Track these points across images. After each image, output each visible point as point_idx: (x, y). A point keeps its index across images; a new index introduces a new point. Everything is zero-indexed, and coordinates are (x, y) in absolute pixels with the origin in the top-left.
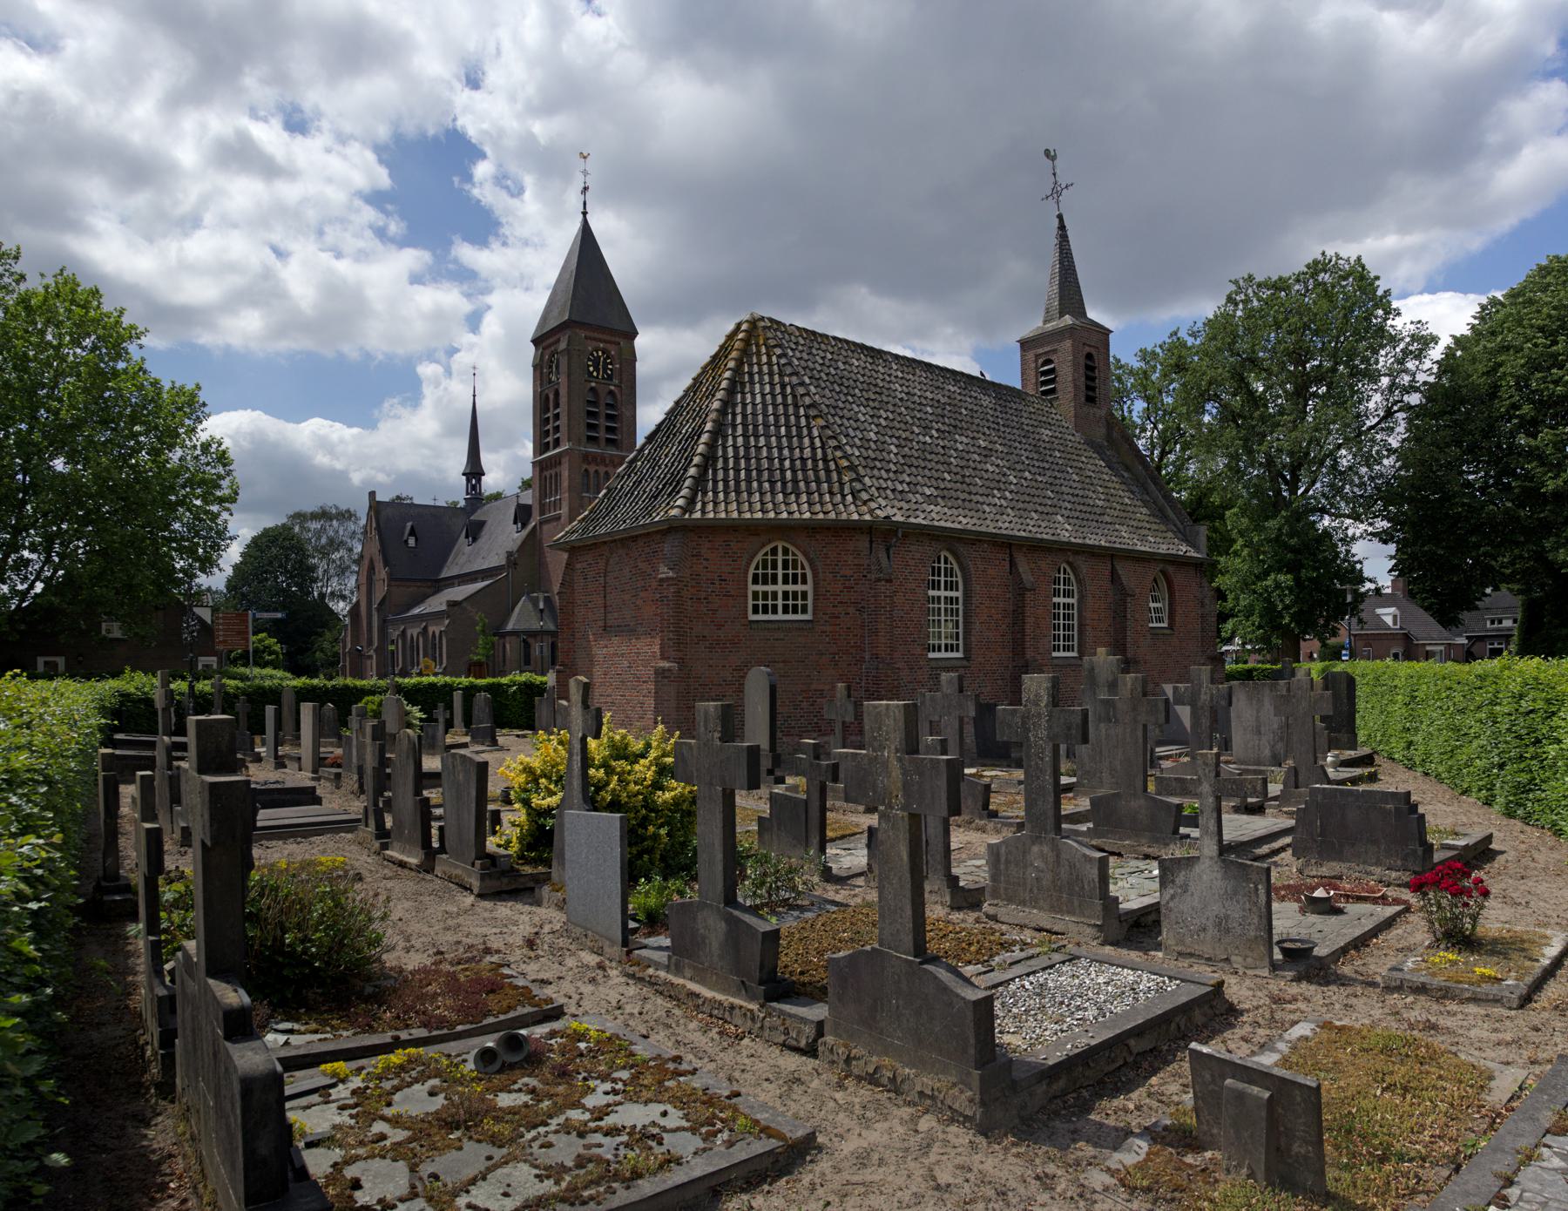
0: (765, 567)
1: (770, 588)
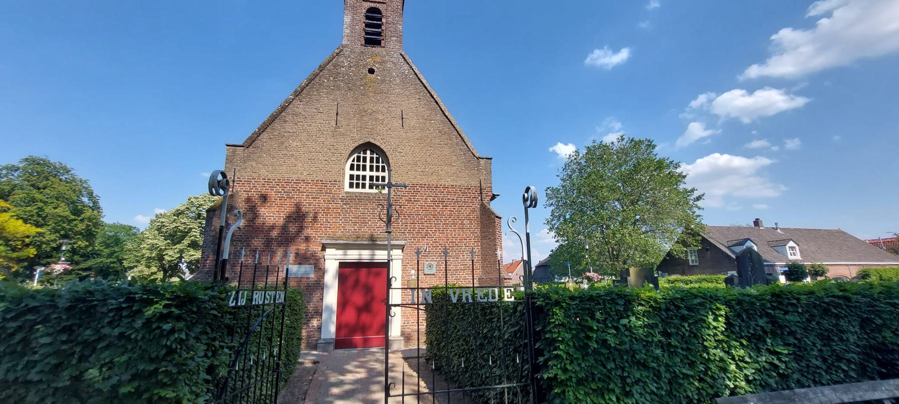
0: (358, 160)
1: (361, 173)
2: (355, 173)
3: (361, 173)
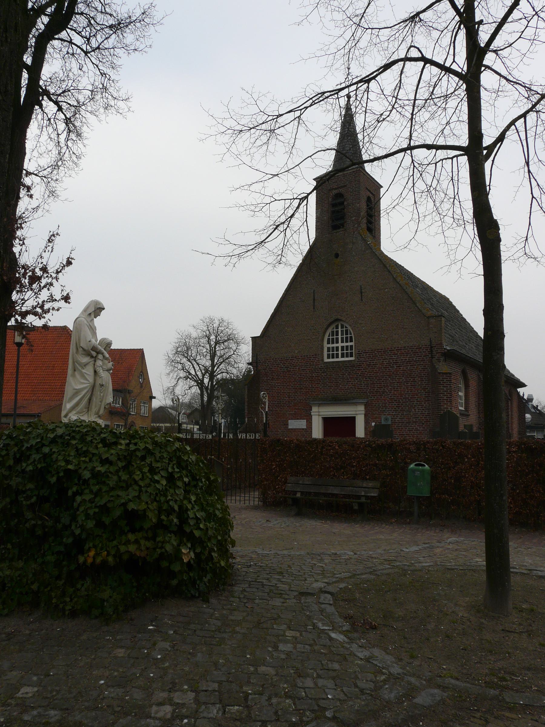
0: (333, 335)
1: (335, 345)
2: (331, 345)
3: (335, 345)
